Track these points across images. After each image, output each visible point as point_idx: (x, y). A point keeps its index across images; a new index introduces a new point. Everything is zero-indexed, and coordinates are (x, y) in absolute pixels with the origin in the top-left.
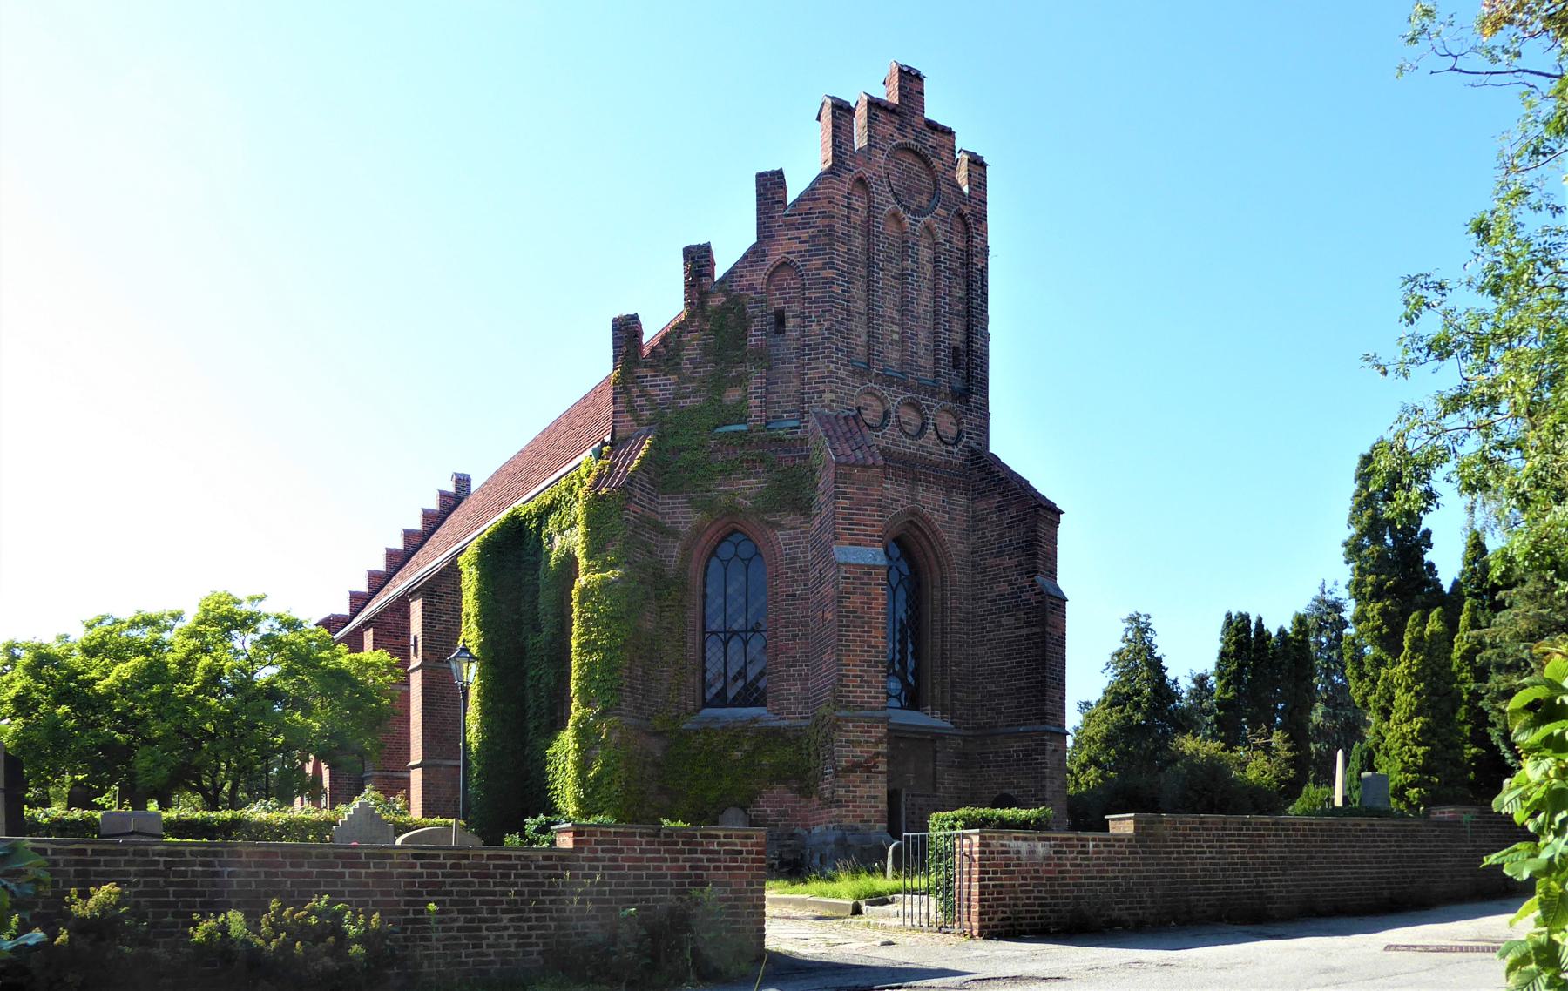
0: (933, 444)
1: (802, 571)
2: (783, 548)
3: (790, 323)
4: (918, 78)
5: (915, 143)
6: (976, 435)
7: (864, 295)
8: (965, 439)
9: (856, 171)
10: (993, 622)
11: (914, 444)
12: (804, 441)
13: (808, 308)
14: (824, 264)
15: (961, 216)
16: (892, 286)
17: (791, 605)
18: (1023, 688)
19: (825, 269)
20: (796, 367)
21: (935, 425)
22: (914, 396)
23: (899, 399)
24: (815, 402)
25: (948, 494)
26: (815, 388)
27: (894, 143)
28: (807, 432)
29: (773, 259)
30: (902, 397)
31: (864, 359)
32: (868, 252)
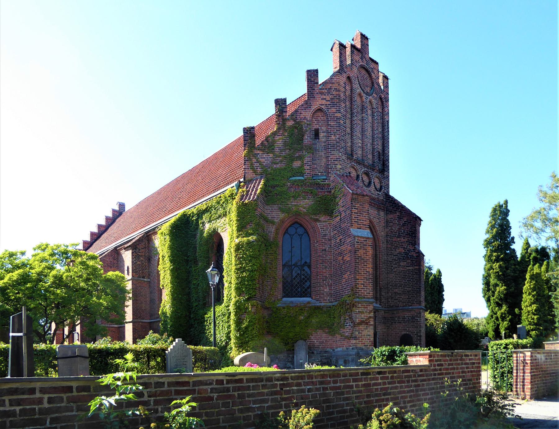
1: (329, 240)
3: (321, 135)
7: (350, 126)
17: (324, 254)
20: (324, 154)
29: (314, 107)
31: (350, 153)
32: (351, 108)
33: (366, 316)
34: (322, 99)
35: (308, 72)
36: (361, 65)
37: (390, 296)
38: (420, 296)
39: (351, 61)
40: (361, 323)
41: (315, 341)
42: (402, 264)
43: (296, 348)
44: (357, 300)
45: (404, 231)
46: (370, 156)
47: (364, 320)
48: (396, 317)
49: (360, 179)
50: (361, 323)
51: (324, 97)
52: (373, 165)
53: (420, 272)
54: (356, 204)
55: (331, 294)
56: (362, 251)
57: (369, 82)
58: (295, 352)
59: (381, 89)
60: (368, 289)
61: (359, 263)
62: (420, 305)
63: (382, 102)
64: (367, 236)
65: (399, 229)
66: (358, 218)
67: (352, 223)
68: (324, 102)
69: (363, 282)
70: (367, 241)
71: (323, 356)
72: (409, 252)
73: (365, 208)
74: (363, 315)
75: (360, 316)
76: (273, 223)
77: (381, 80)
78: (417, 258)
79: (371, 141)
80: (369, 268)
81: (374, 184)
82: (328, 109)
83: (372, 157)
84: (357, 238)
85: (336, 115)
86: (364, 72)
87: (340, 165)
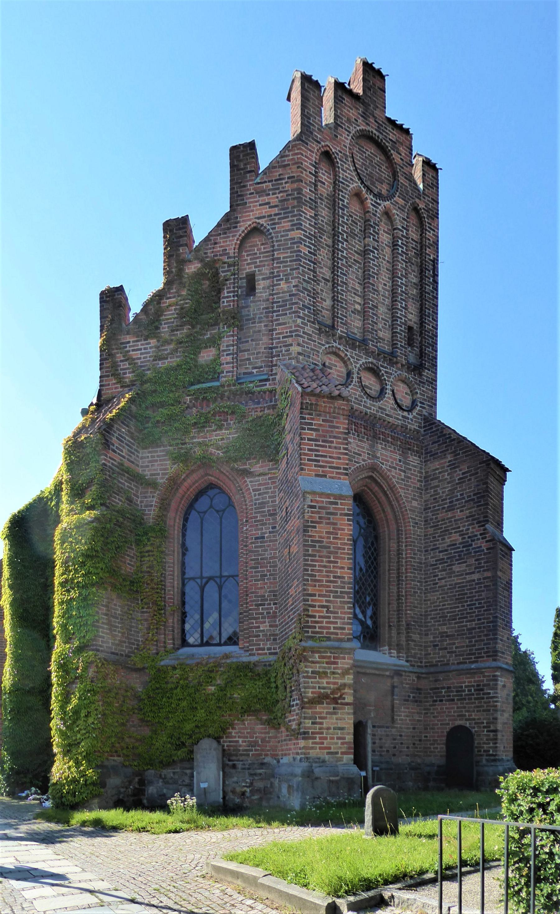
0: (391, 408)
1: (271, 515)
2: (253, 493)
3: (261, 285)
7: (329, 263)
9: (323, 143)
11: (374, 406)
14: (292, 225)
16: (354, 260)
17: (261, 547)
19: (293, 230)
20: (265, 326)
21: (393, 391)
22: (375, 361)
23: (361, 362)
24: (283, 355)
30: (364, 361)
31: (329, 322)
32: (334, 225)
33: (335, 683)
34: (260, 205)
35: (234, 150)
36: (362, 131)
37: (431, 642)
38: (496, 639)
39: (335, 119)
40: (320, 699)
41: (240, 740)
42: (456, 568)
43: (198, 757)
44: (310, 643)
45: (461, 495)
46: (385, 334)
47: (329, 691)
48: (443, 688)
49: (355, 379)
50: (320, 699)
51: (266, 199)
52: (392, 353)
53: (495, 584)
54: (312, 419)
55: (274, 635)
56: (322, 530)
57: (385, 173)
58: (195, 764)
59: (418, 190)
60: (340, 618)
61: (314, 556)
62: (495, 660)
63: (420, 219)
64: (338, 492)
65: (452, 491)
66: (317, 451)
67: (301, 464)
68: (266, 210)
69: (327, 601)
70: (336, 503)
71: (255, 774)
72: (472, 541)
73: (338, 427)
74: (325, 681)
75: (318, 683)
76: (153, 485)
77: (418, 174)
78: (490, 553)
79: (388, 302)
80: (343, 568)
81: (394, 395)
82: (274, 224)
83: (390, 336)
84: (309, 497)
85: (291, 234)
87: (299, 345)
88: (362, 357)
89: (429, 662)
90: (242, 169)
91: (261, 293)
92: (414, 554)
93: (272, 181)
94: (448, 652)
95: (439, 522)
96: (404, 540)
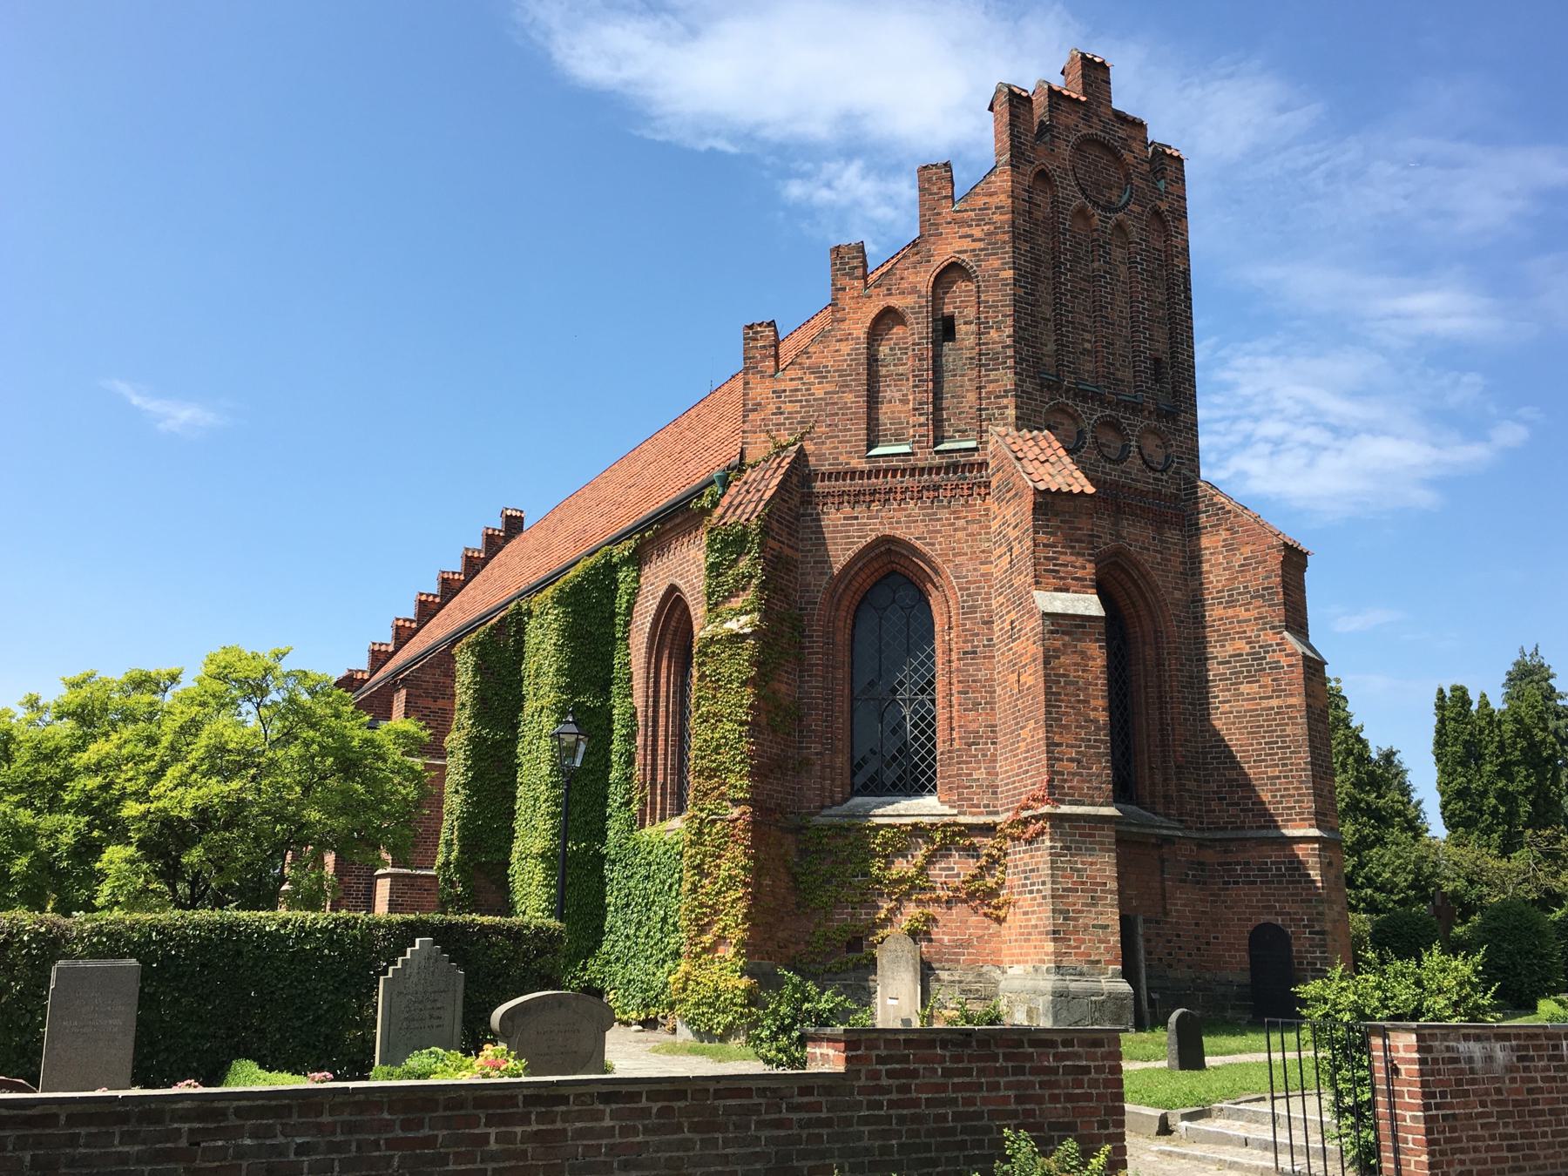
2: (959, 594)
3: (961, 329)
4: (1103, 67)
5: (1103, 134)
6: (1189, 459)
8: (1175, 465)
10: (1229, 690)
11: (1115, 470)
12: (983, 465)
13: (984, 312)
15: (1157, 213)
16: (1081, 289)
18: (1279, 777)
20: (970, 380)
22: (1113, 413)
23: (1095, 417)
24: (996, 419)
25: (1159, 530)
26: (995, 403)
27: (1079, 134)
28: (986, 455)
29: (940, 259)
30: (1099, 415)
37: (1214, 792)
86: (1093, 153)
88: (1096, 410)
89: (1213, 823)
90: (935, 194)
91: (963, 339)
92: (1181, 665)
93: (975, 210)
94: (1242, 810)
95: (1214, 621)
96: (1165, 645)
